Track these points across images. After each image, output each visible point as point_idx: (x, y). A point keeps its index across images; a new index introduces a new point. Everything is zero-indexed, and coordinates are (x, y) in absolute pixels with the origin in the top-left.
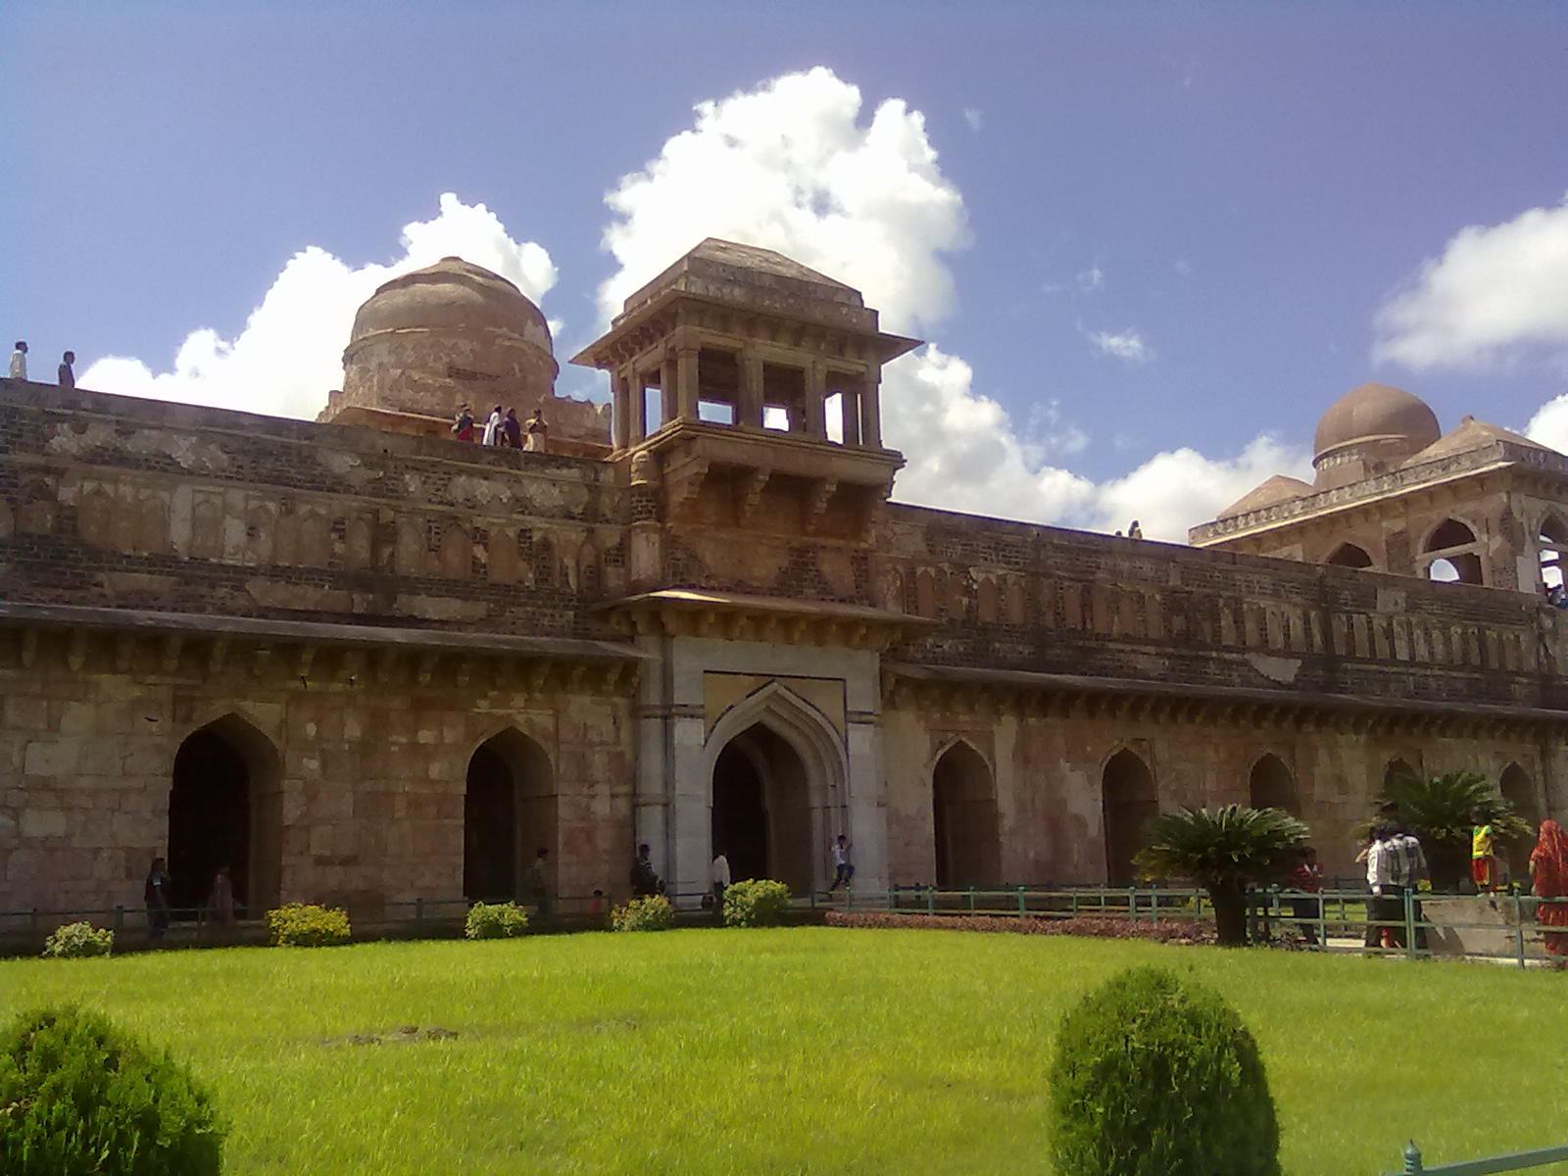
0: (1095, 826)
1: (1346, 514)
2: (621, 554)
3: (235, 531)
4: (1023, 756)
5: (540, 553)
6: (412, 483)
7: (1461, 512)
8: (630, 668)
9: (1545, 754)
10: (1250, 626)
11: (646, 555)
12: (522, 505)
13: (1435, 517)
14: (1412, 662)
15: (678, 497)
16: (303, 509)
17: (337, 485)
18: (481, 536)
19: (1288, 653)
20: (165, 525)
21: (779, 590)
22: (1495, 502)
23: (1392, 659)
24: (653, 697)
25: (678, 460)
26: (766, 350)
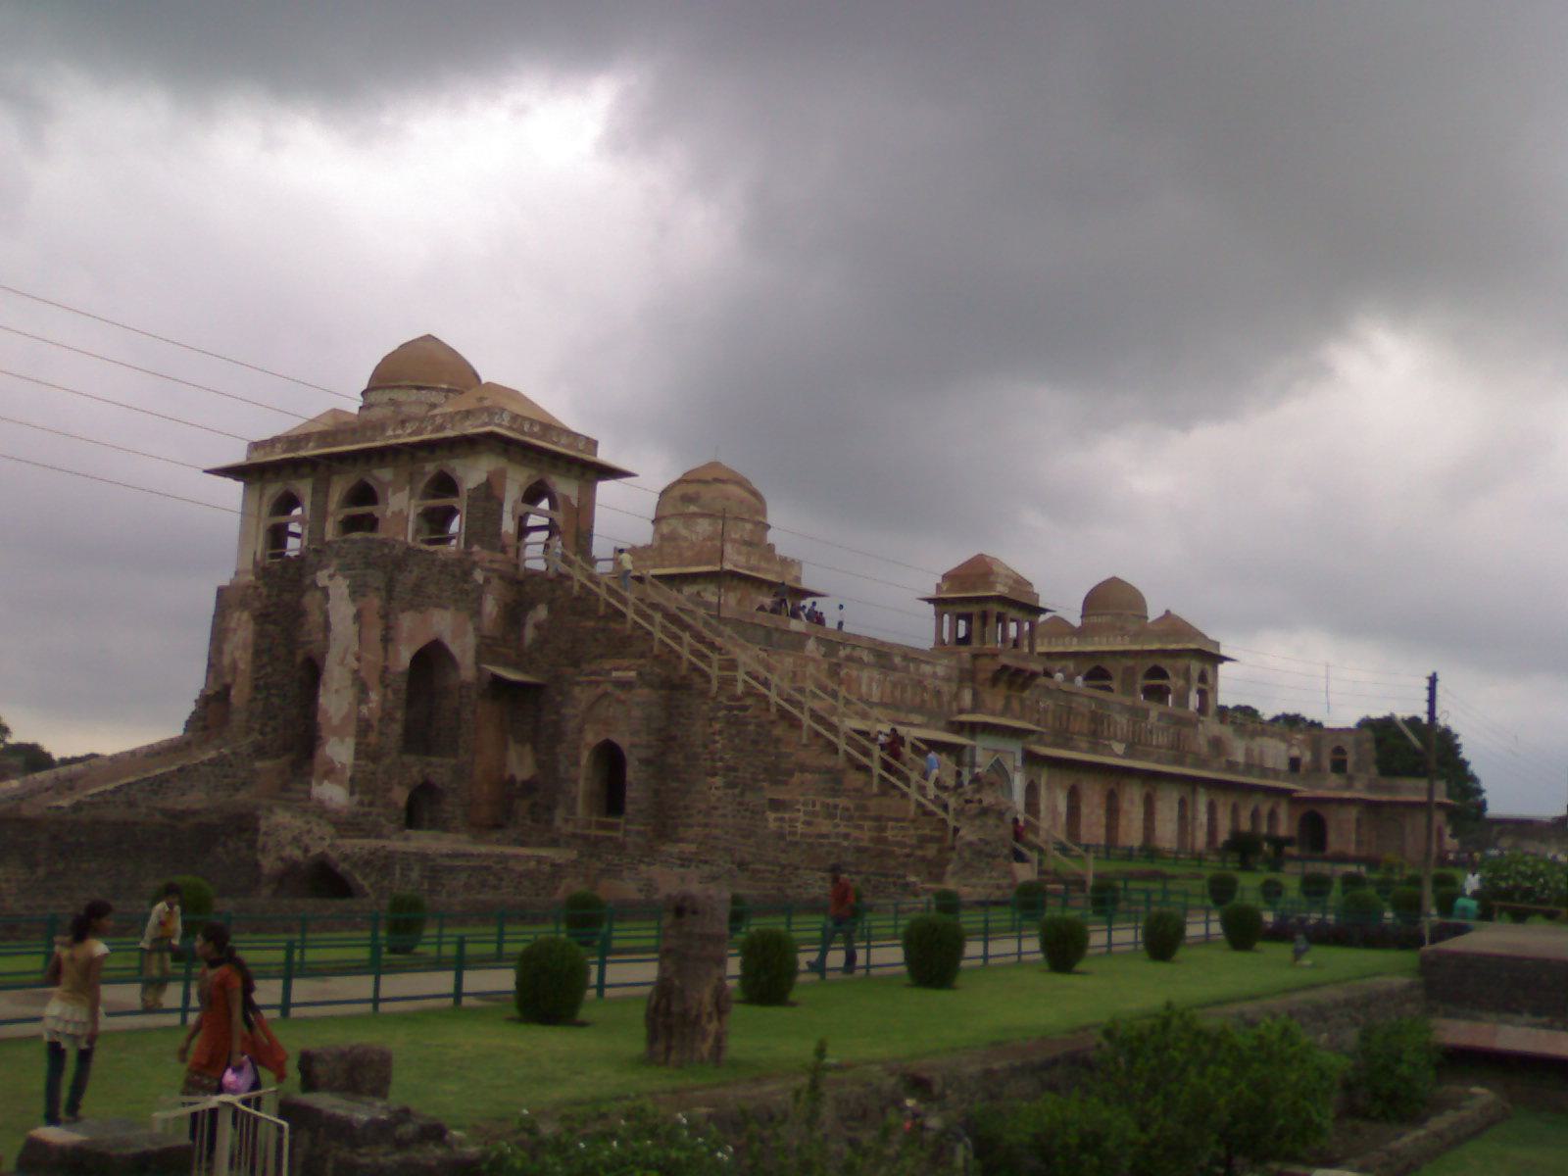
0: (1064, 818)
1: (1103, 653)
2: (957, 696)
3: (874, 686)
4: (1049, 788)
5: (938, 693)
6: (912, 666)
7: (1165, 664)
8: (962, 747)
9: (1194, 791)
10: (1111, 729)
11: (967, 697)
12: (935, 675)
13: (1150, 663)
14: (1158, 747)
15: (981, 676)
16: (888, 679)
17: (895, 669)
18: (925, 689)
19: (1121, 741)
20: (860, 686)
21: (1003, 714)
22: (1181, 663)
23: (1151, 745)
24: (967, 759)
25: (984, 662)
26: (1013, 613)
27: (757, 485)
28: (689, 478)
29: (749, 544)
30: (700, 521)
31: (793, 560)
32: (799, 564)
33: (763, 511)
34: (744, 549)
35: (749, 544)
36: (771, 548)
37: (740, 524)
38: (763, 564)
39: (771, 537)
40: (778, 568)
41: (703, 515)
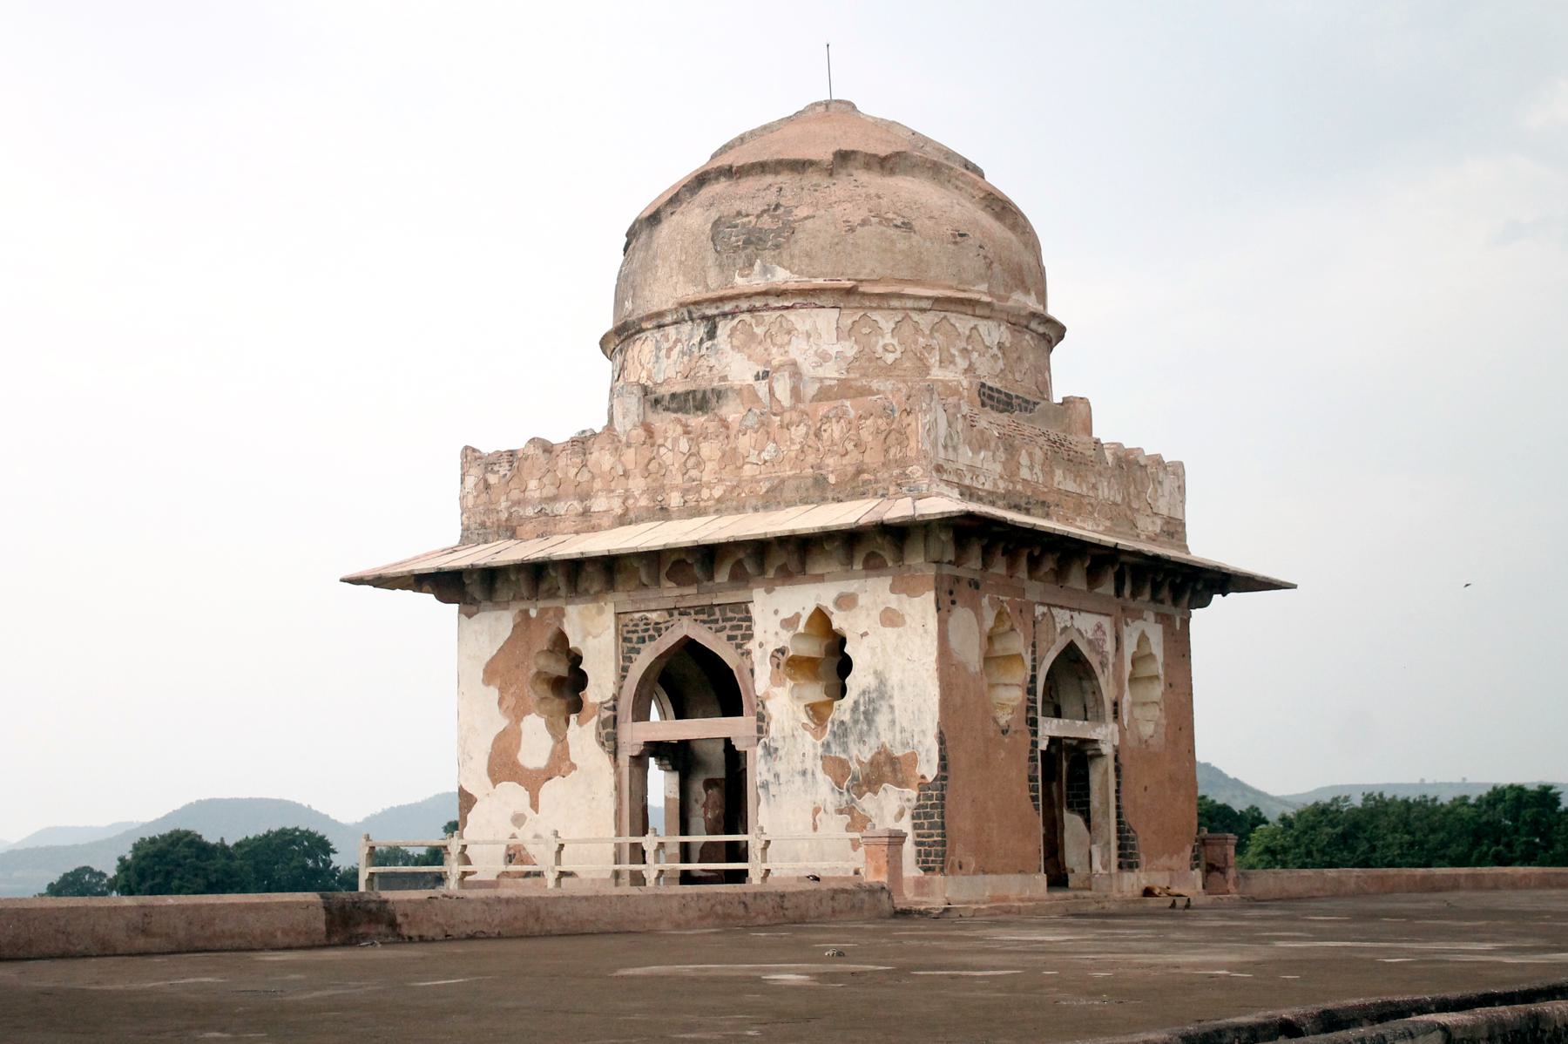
27: (998, 178)
28: (735, 159)
29: (991, 398)
30: (801, 319)
31: (1157, 460)
32: (1177, 470)
33: (1031, 277)
34: (991, 422)
35: (991, 398)
36: (1076, 412)
37: (963, 323)
38: (1063, 481)
39: (1068, 373)
40: (1107, 491)
41: (809, 296)
